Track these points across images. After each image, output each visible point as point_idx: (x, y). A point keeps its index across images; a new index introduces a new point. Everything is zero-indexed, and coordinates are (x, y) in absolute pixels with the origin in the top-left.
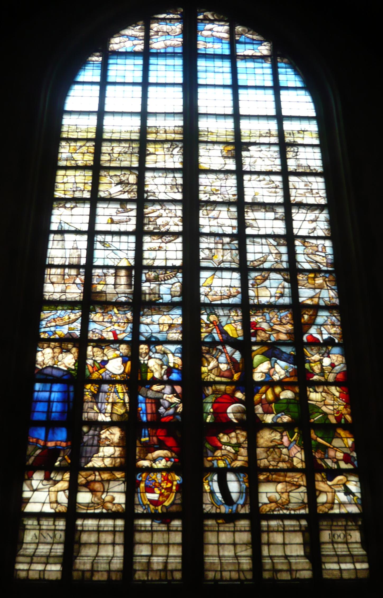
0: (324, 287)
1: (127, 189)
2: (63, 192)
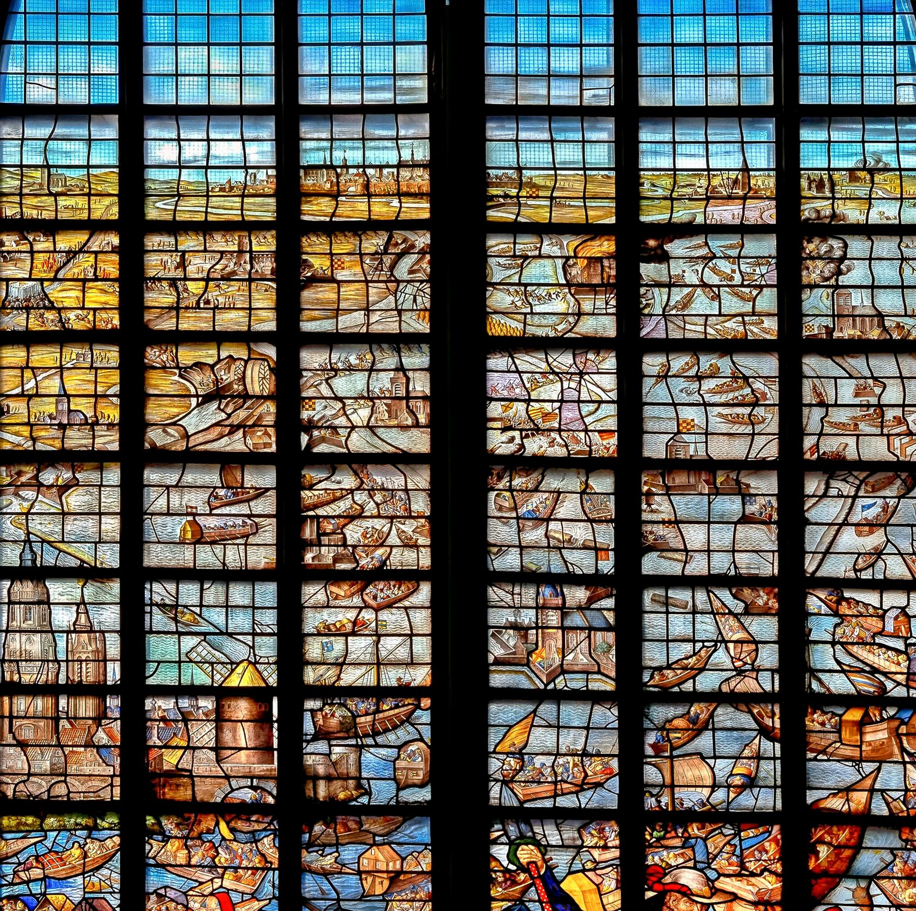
0: (891, 755)
1: (242, 414)
2: (25, 430)
